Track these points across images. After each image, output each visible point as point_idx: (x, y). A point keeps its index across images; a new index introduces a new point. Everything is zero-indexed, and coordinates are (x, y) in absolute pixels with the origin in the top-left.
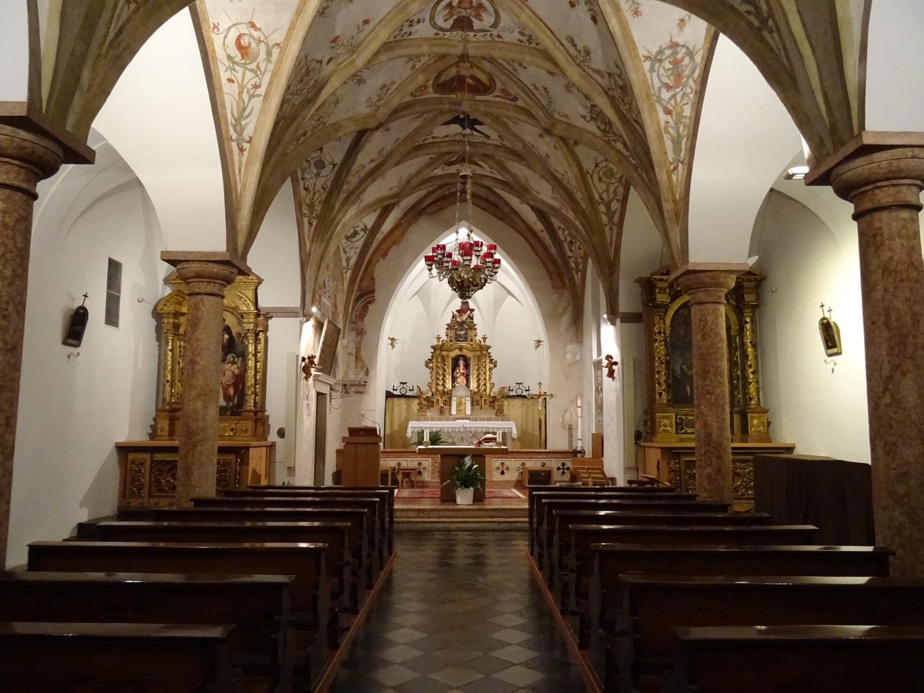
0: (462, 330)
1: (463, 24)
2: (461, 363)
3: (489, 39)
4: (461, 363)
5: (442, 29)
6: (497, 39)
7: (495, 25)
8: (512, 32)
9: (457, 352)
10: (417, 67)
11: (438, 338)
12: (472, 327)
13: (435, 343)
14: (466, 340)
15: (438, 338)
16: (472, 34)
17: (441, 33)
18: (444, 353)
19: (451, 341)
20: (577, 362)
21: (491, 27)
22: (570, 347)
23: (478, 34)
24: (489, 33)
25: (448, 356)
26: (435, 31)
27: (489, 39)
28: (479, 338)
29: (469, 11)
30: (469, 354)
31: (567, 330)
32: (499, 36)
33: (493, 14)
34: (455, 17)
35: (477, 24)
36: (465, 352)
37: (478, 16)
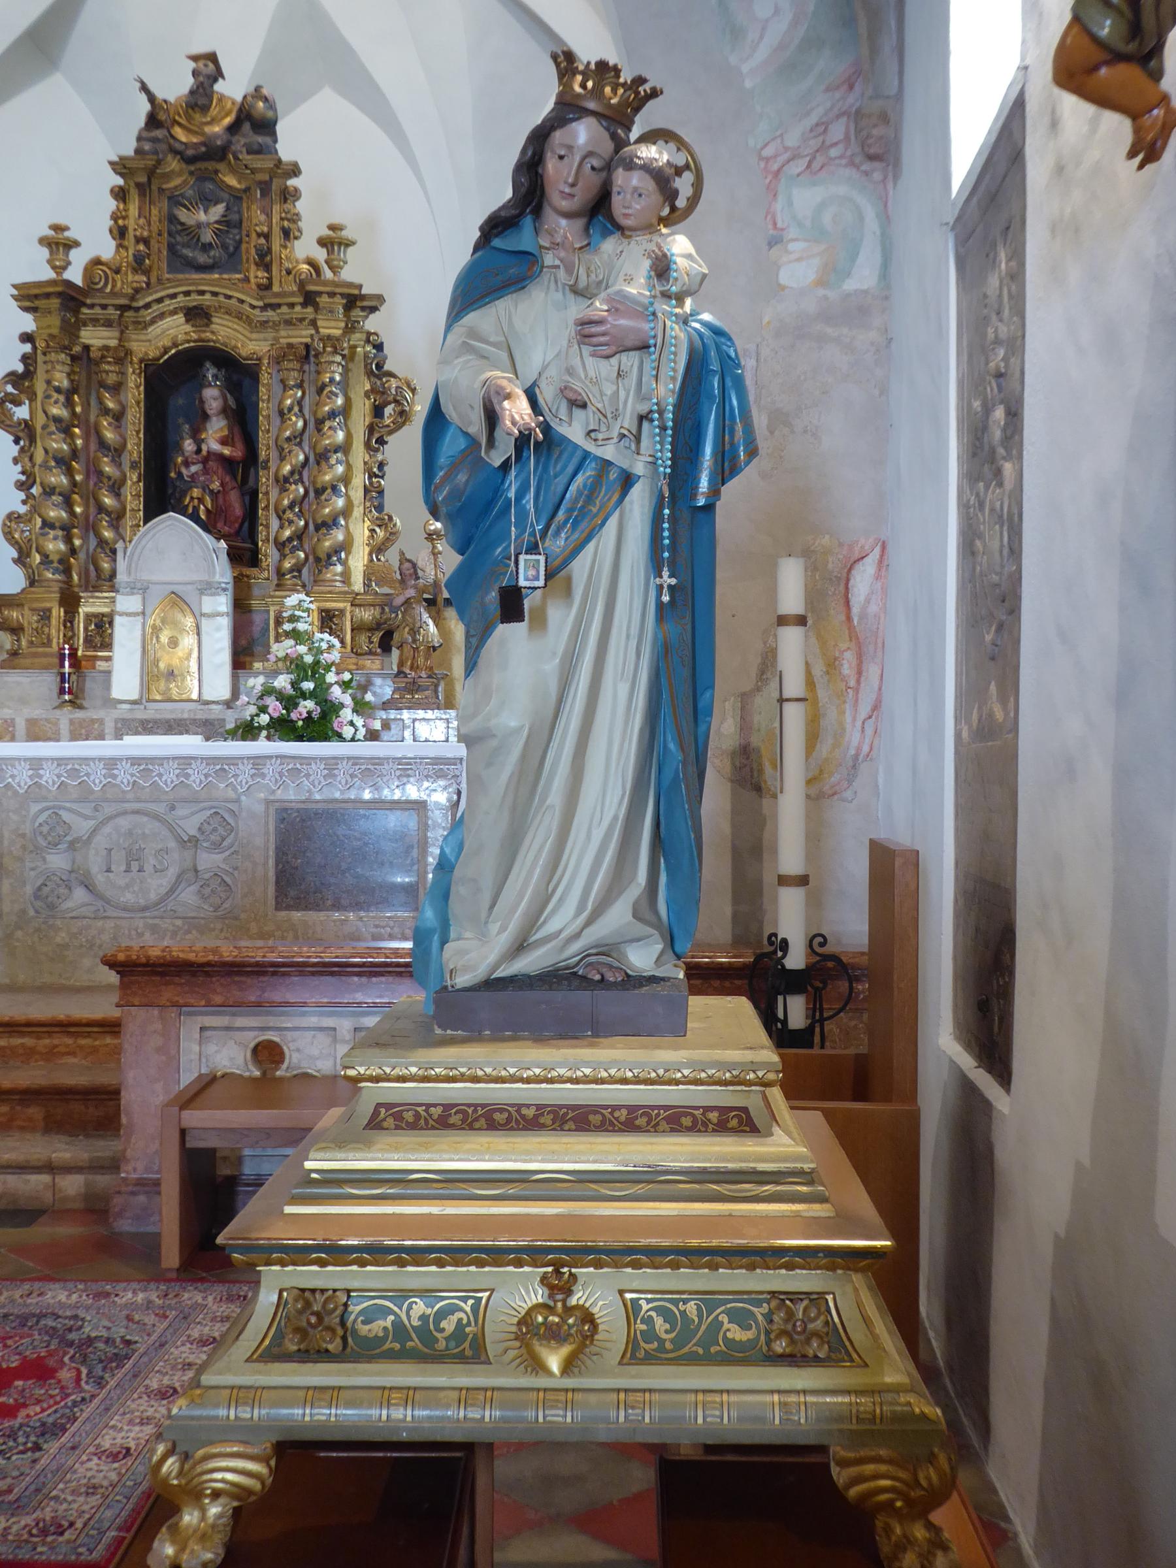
0: (207, 201)
2: (213, 397)
4: (213, 397)
9: (169, 332)
11: (58, 243)
12: (277, 182)
13: (37, 268)
14: (231, 260)
15: (58, 243)
18: (94, 337)
19: (139, 264)
20: (857, 311)
22: (804, 199)
25: (122, 356)
28: (307, 247)
30: (250, 344)
31: (789, 67)
36: (225, 332)
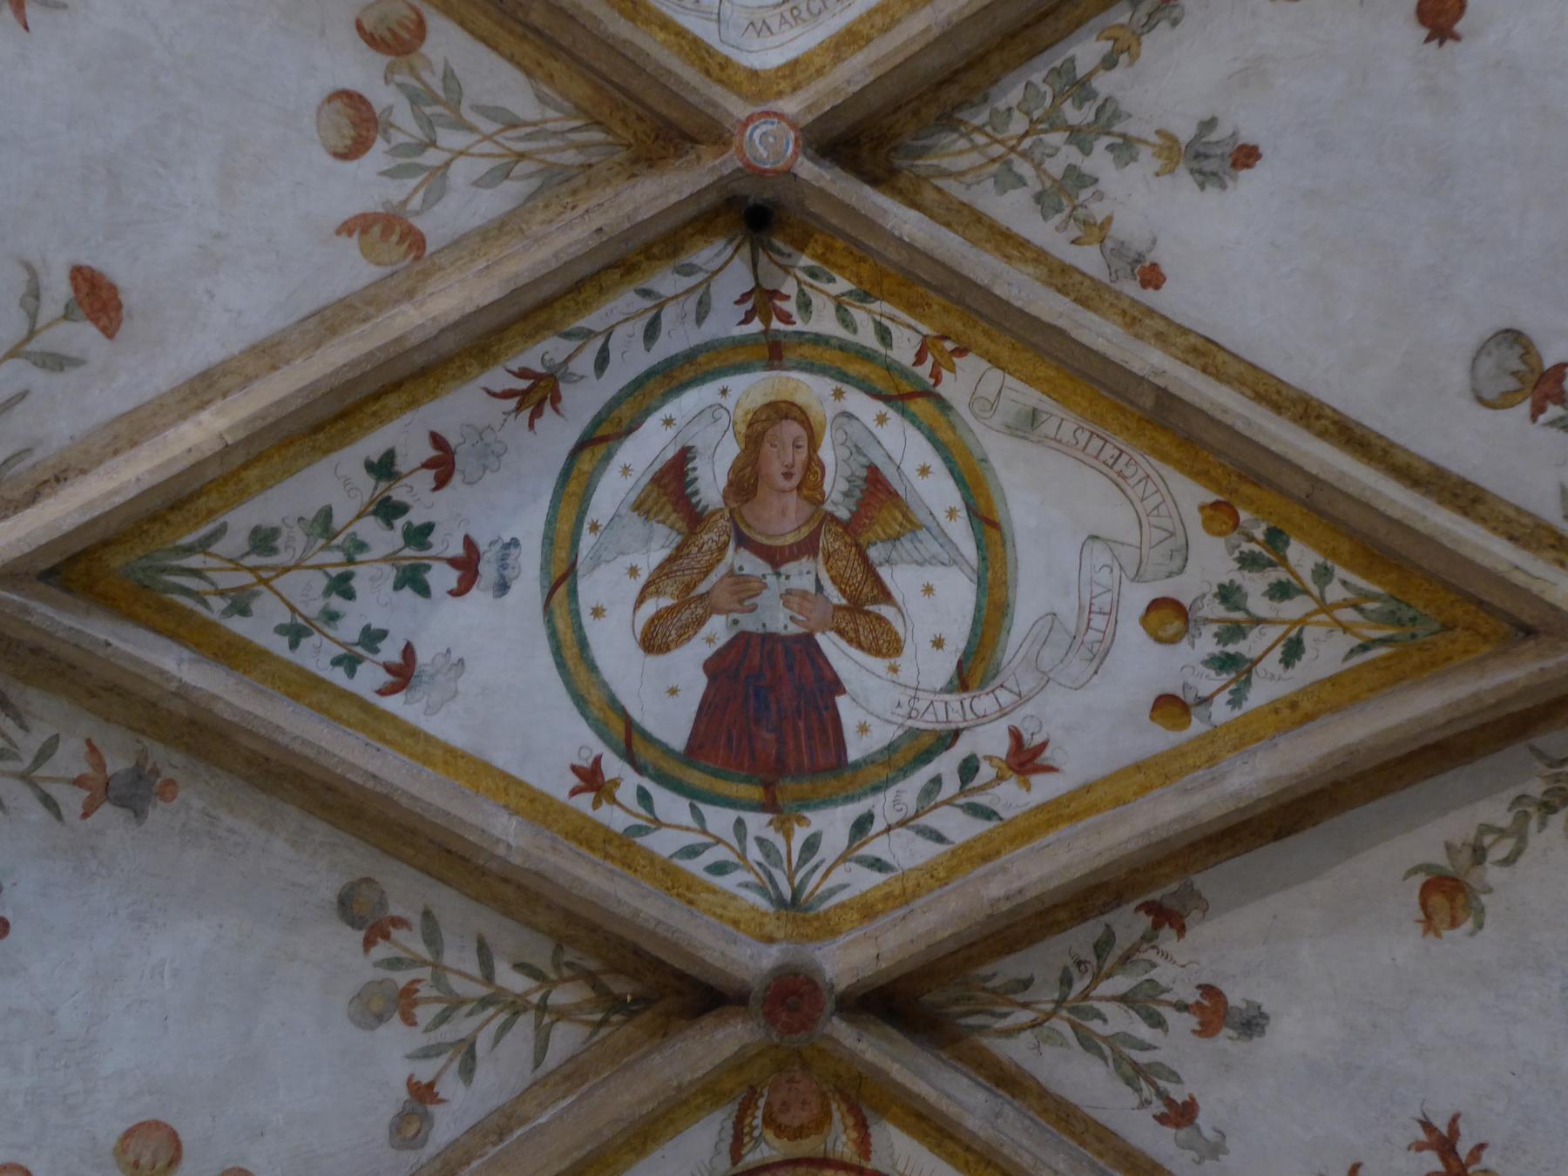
1: (769, 724)
3: (959, 827)
5: (630, 740)
6: (1012, 798)
7: (971, 673)
8: (1099, 657)
10: (447, 1125)
16: (832, 824)
17: (630, 783)
21: (965, 679)
23: (884, 806)
24: (946, 765)
26: (579, 740)
27: (959, 827)
29: (801, 574)
32: (1025, 759)
33: (960, 532)
34: (718, 630)
35: (872, 702)
37: (866, 614)
